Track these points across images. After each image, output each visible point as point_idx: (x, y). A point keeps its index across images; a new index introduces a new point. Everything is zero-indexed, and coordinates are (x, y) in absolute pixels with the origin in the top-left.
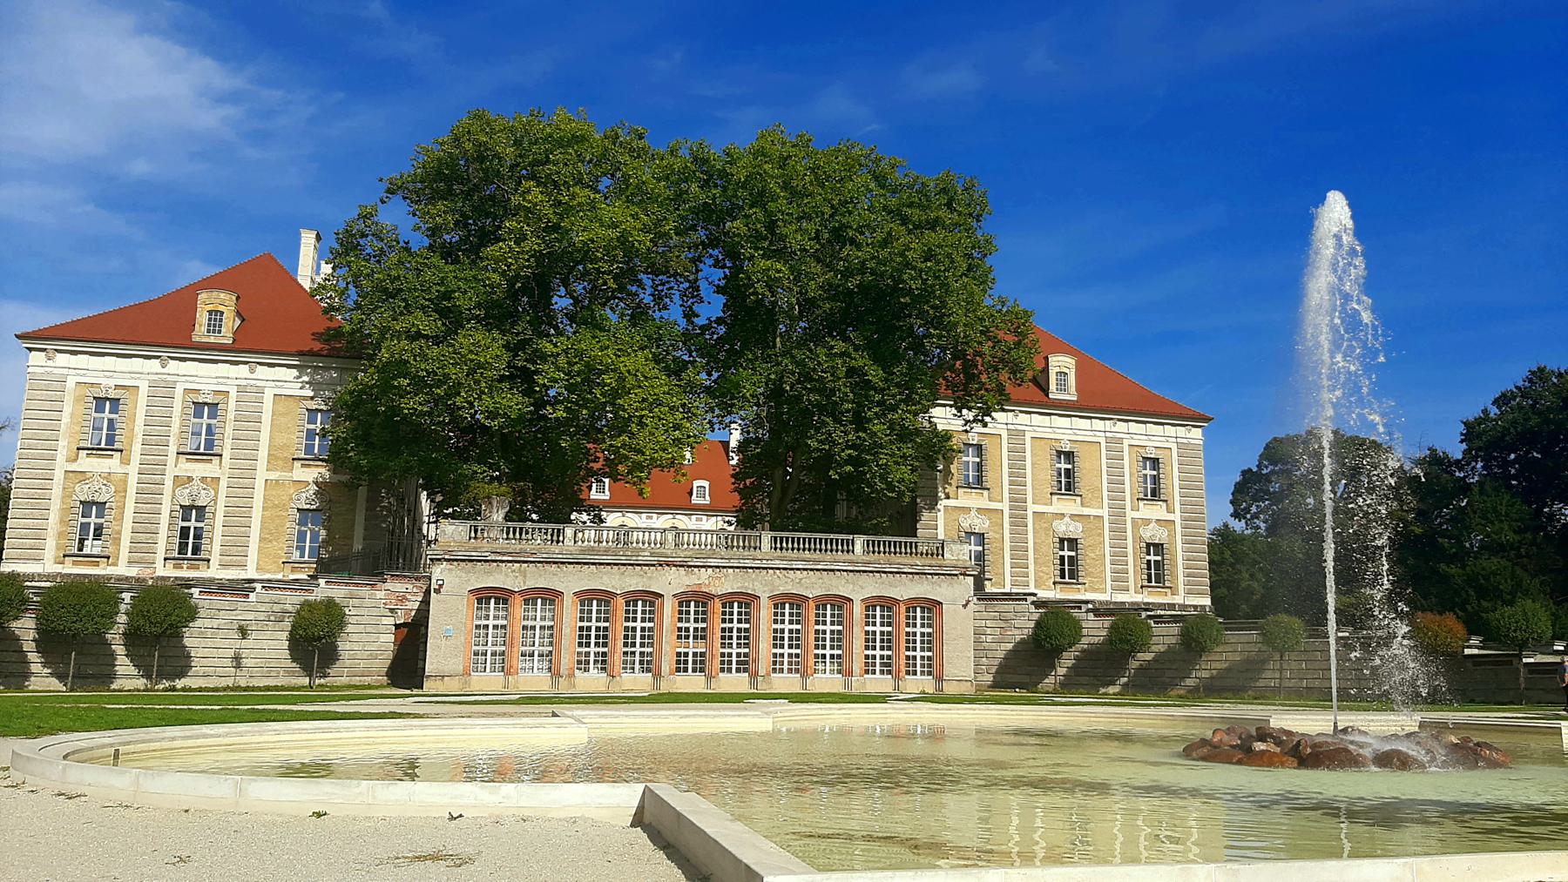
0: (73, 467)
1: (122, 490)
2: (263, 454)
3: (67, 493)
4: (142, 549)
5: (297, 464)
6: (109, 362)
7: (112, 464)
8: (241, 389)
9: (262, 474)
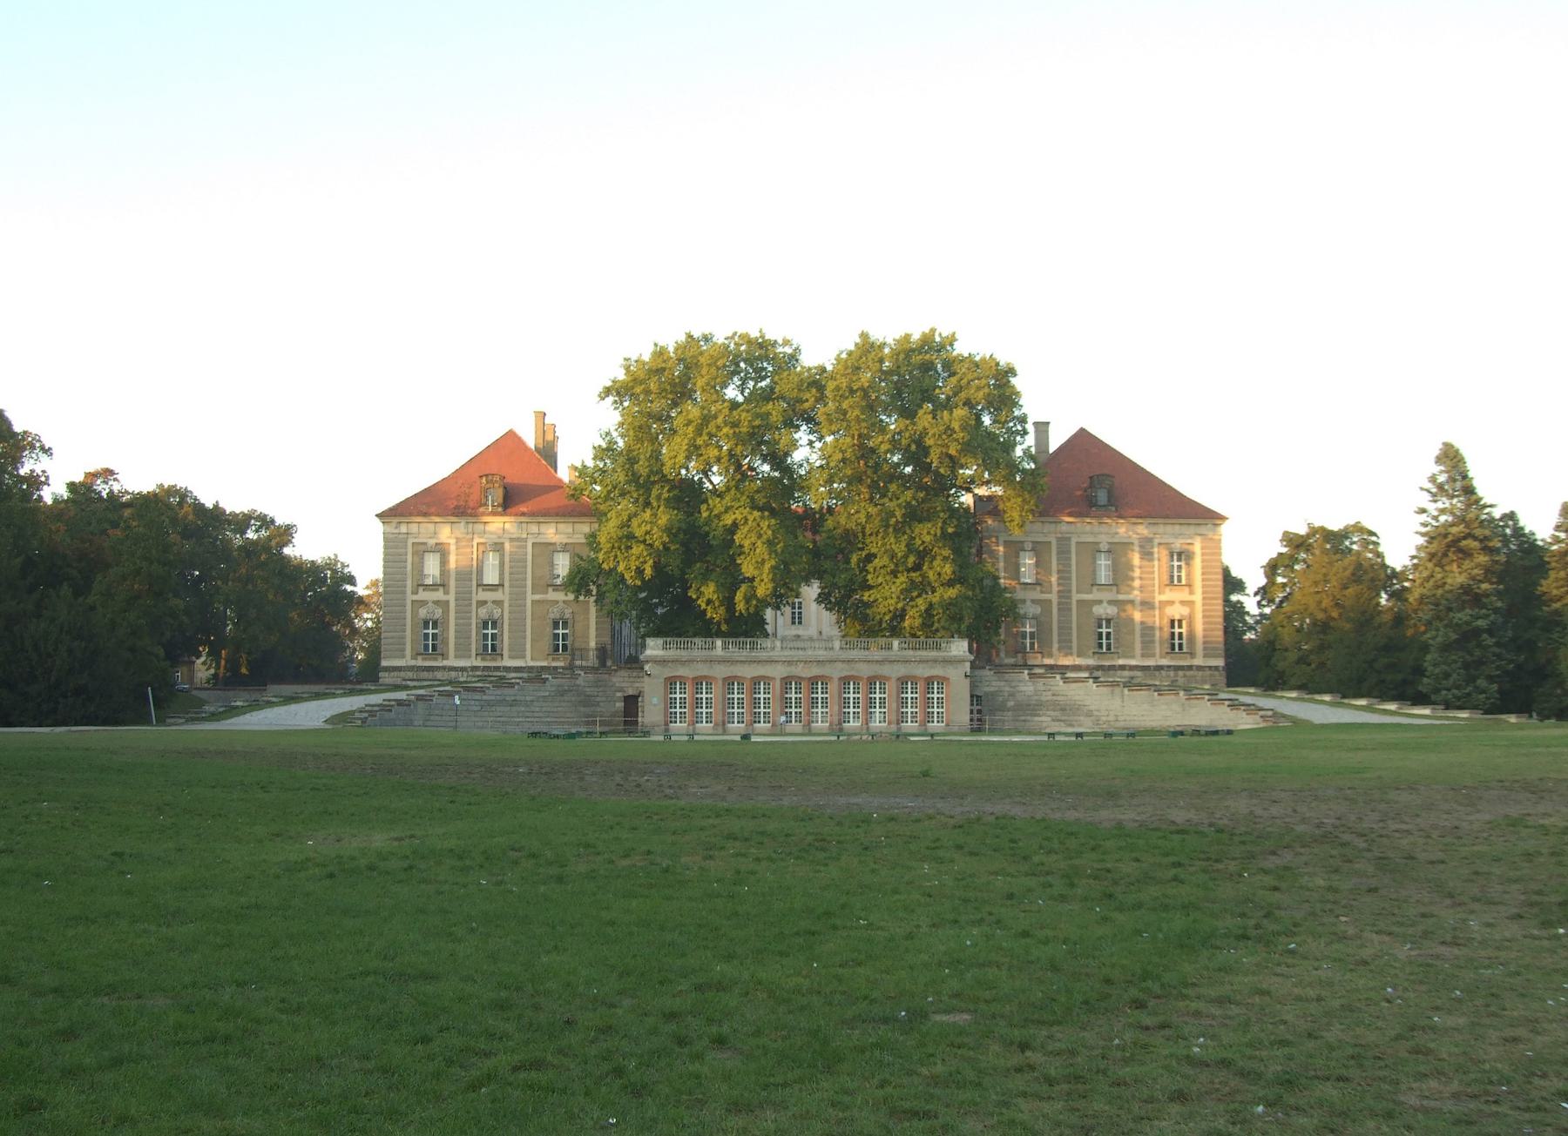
0: (415, 597)
1: (446, 612)
2: (529, 583)
3: (414, 614)
4: (462, 652)
7: (439, 595)
9: (530, 597)
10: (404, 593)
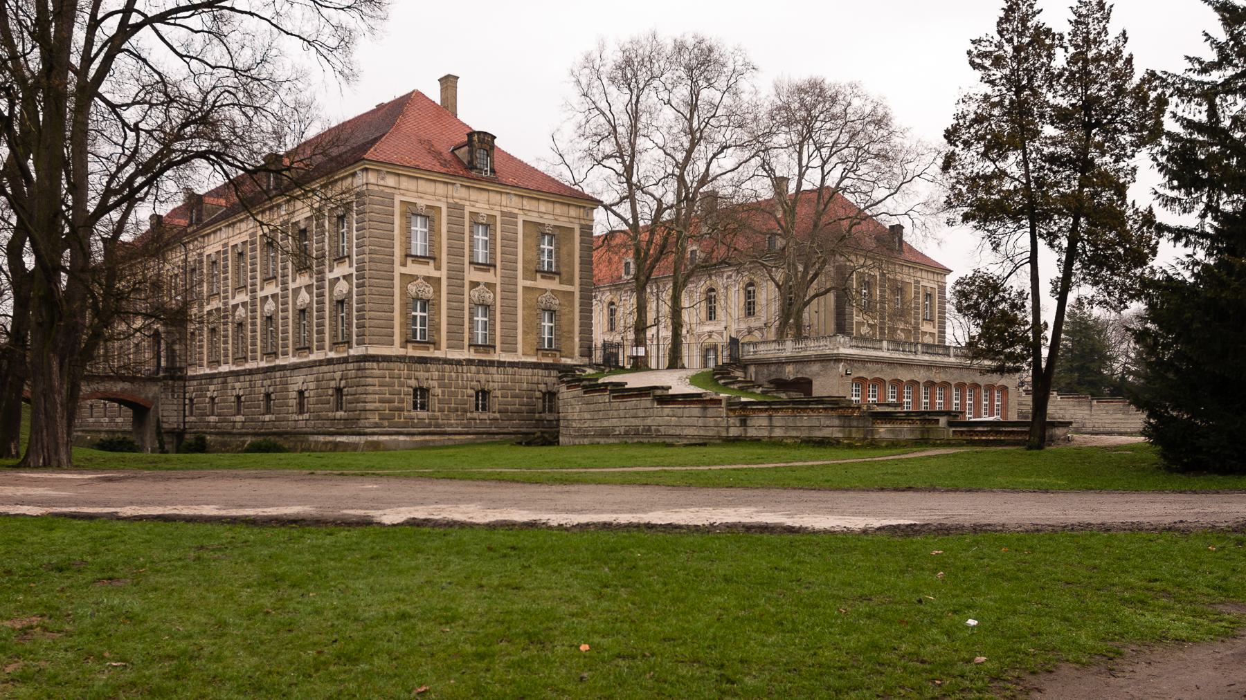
0: (404, 270)
1: (438, 291)
2: (520, 266)
3: (404, 292)
5: (539, 276)
6: (424, 186)
7: (428, 270)
8: (503, 214)
9: (521, 283)
10: (392, 263)
